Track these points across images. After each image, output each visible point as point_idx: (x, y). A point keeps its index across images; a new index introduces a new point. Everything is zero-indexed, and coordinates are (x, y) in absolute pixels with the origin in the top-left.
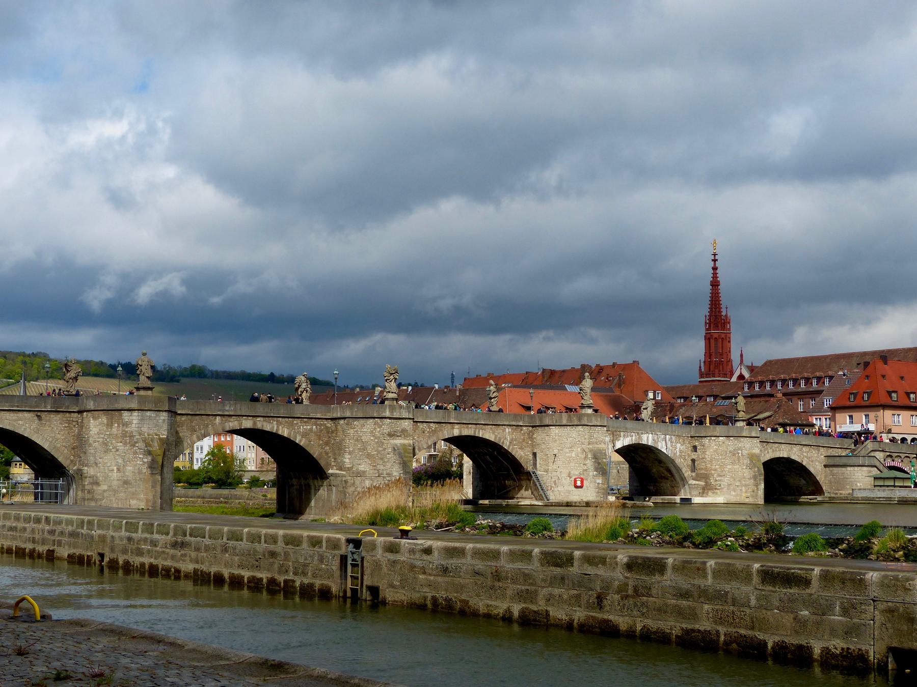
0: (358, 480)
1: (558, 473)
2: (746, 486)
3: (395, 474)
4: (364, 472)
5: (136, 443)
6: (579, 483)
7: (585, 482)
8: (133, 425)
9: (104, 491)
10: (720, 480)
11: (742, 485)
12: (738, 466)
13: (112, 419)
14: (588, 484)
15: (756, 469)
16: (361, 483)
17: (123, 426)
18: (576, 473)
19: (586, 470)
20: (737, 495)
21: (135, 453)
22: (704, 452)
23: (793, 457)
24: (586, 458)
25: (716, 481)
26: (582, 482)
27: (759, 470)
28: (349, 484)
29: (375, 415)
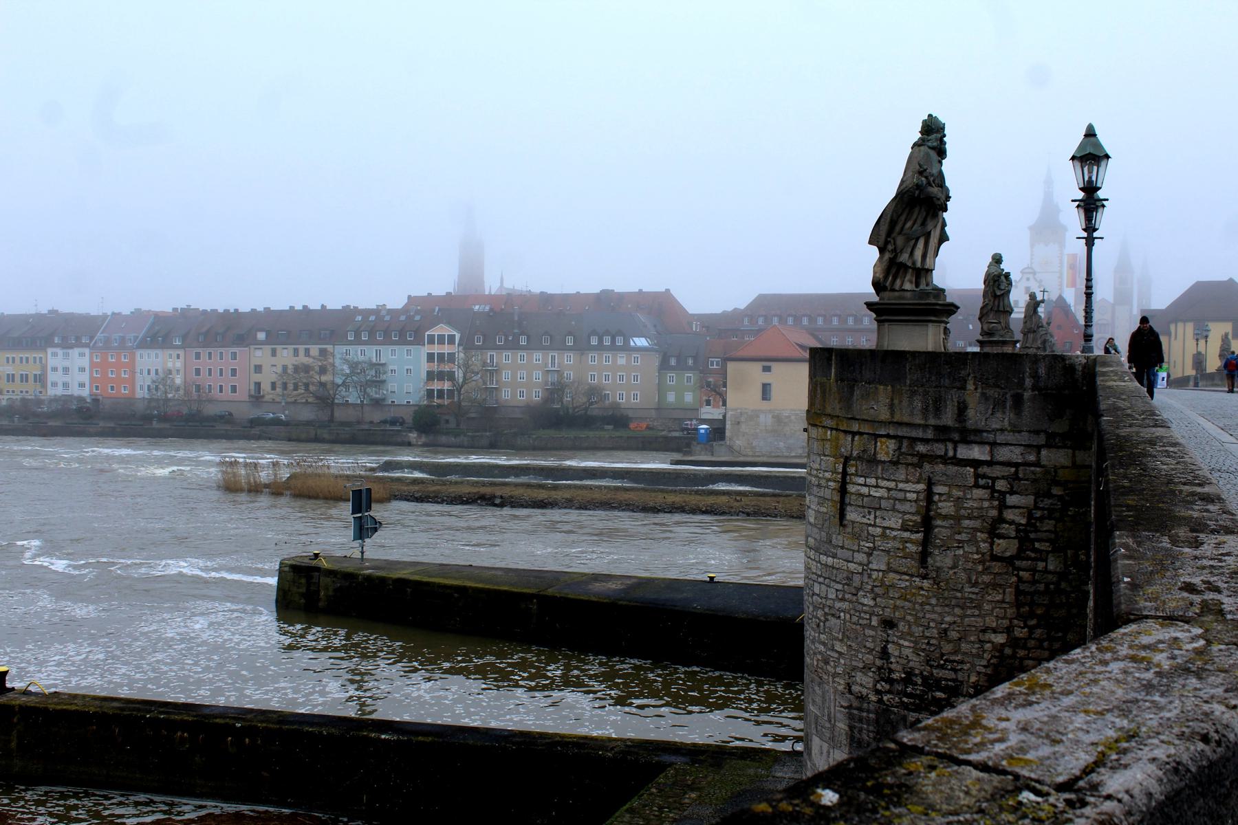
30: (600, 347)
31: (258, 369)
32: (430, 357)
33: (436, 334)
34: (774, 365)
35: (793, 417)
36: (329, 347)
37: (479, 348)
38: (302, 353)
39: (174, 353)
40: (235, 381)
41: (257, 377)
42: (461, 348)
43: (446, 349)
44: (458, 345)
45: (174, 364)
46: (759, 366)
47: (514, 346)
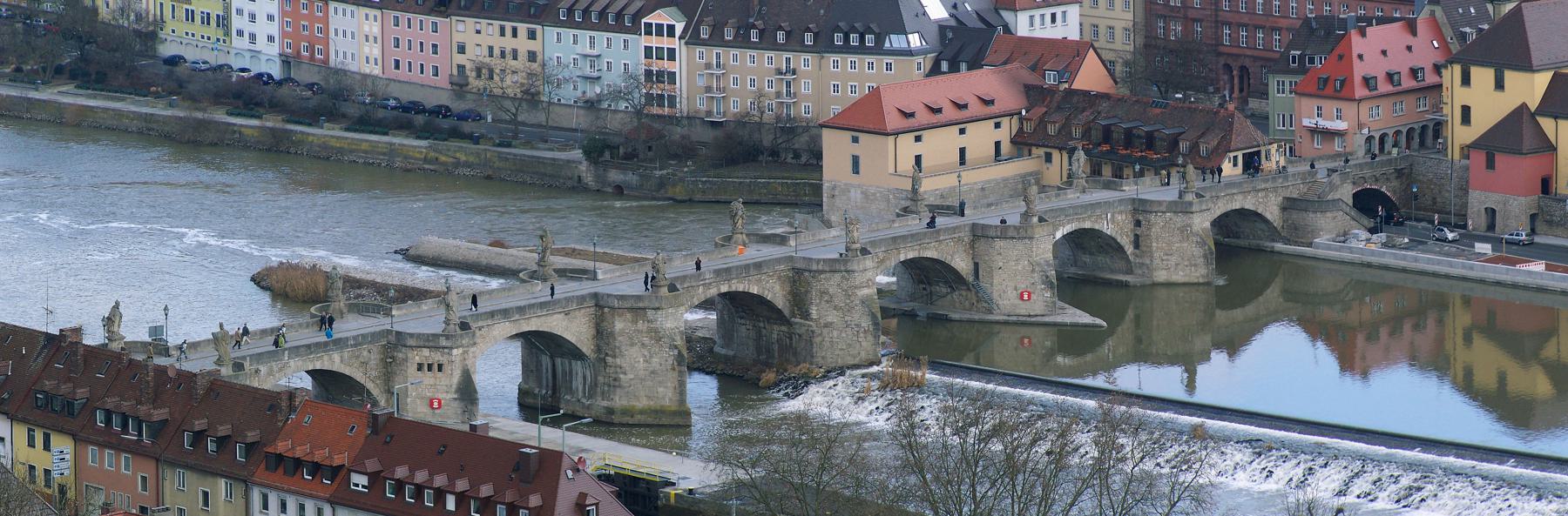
0: (825, 331)
1: (1004, 286)
2: (1195, 265)
4: (831, 323)
6: (1026, 297)
7: (1032, 295)
9: (631, 379)
10: (1168, 260)
11: (1191, 265)
13: (637, 316)
14: (1035, 298)
15: (1206, 247)
16: (828, 333)
17: (648, 322)
18: (1022, 287)
20: (1186, 275)
22: (1149, 229)
23: (1246, 207)
24: (1033, 271)
25: (1163, 260)
27: (1210, 248)
28: (815, 335)
30: (846, 49)
31: (462, 49)
32: (648, 50)
33: (654, 22)
34: (862, 136)
35: (878, 195)
36: (538, 28)
37: (704, 43)
38: (508, 32)
39: (372, 12)
40: (436, 60)
41: (459, 59)
42: (683, 41)
43: (665, 42)
44: (680, 38)
45: (371, 28)
46: (848, 135)
47: (742, 41)
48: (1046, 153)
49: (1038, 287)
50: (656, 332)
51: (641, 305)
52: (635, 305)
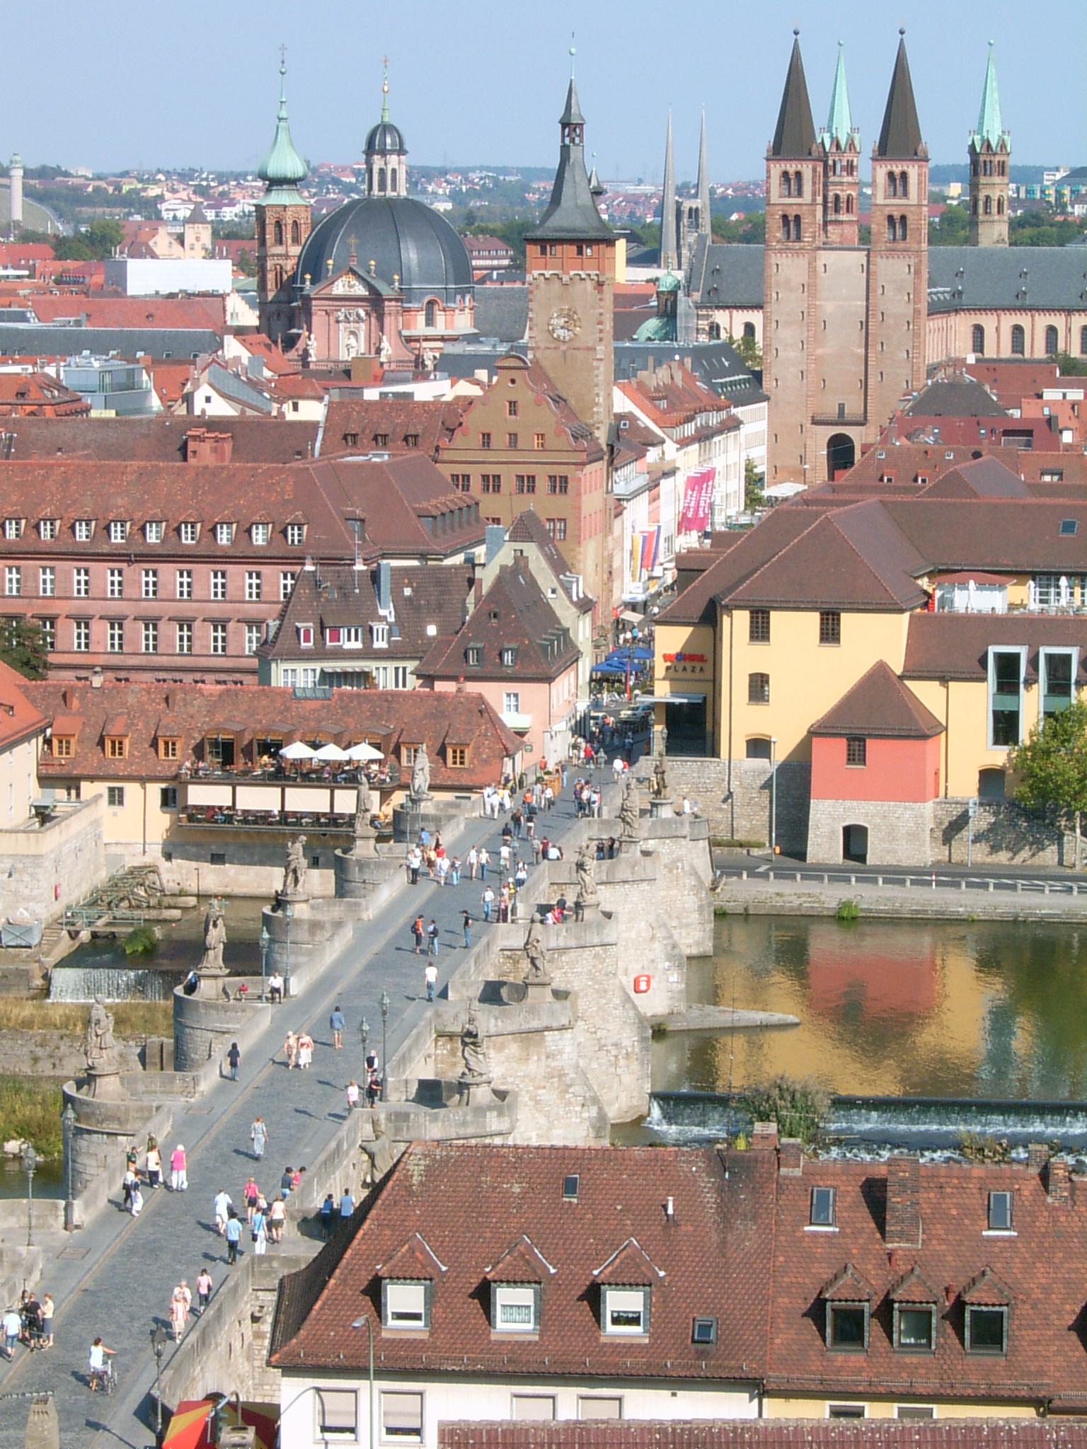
2: (688, 925)
3: (626, 1043)
5: (570, 1086)
8: (565, 1056)
12: (675, 892)
19: (653, 961)
21: (569, 1103)
24: (653, 938)
26: (648, 982)
29: (596, 941)
48: (111, 790)
49: (660, 966)
50: (560, 1076)
51: (535, 1024)
52: (525, 1027)
